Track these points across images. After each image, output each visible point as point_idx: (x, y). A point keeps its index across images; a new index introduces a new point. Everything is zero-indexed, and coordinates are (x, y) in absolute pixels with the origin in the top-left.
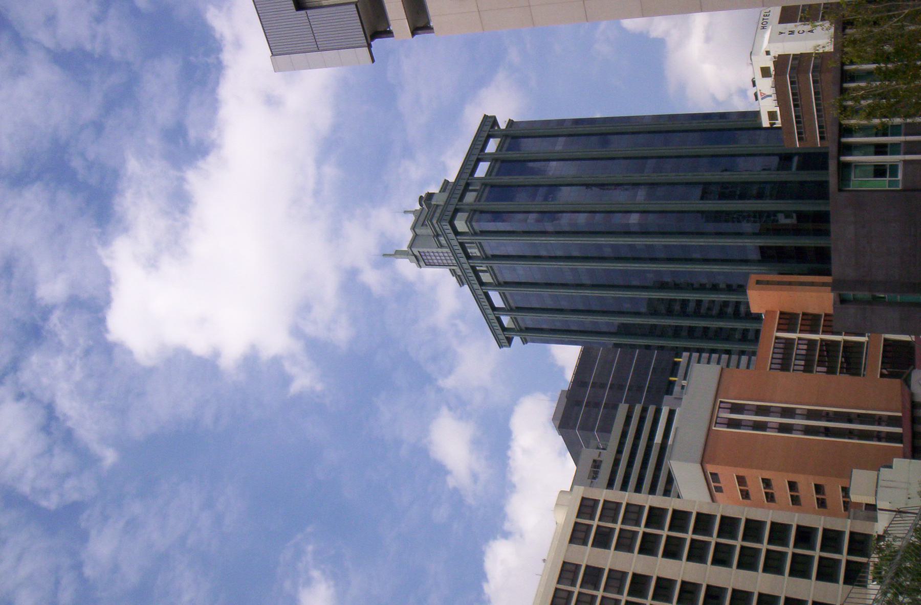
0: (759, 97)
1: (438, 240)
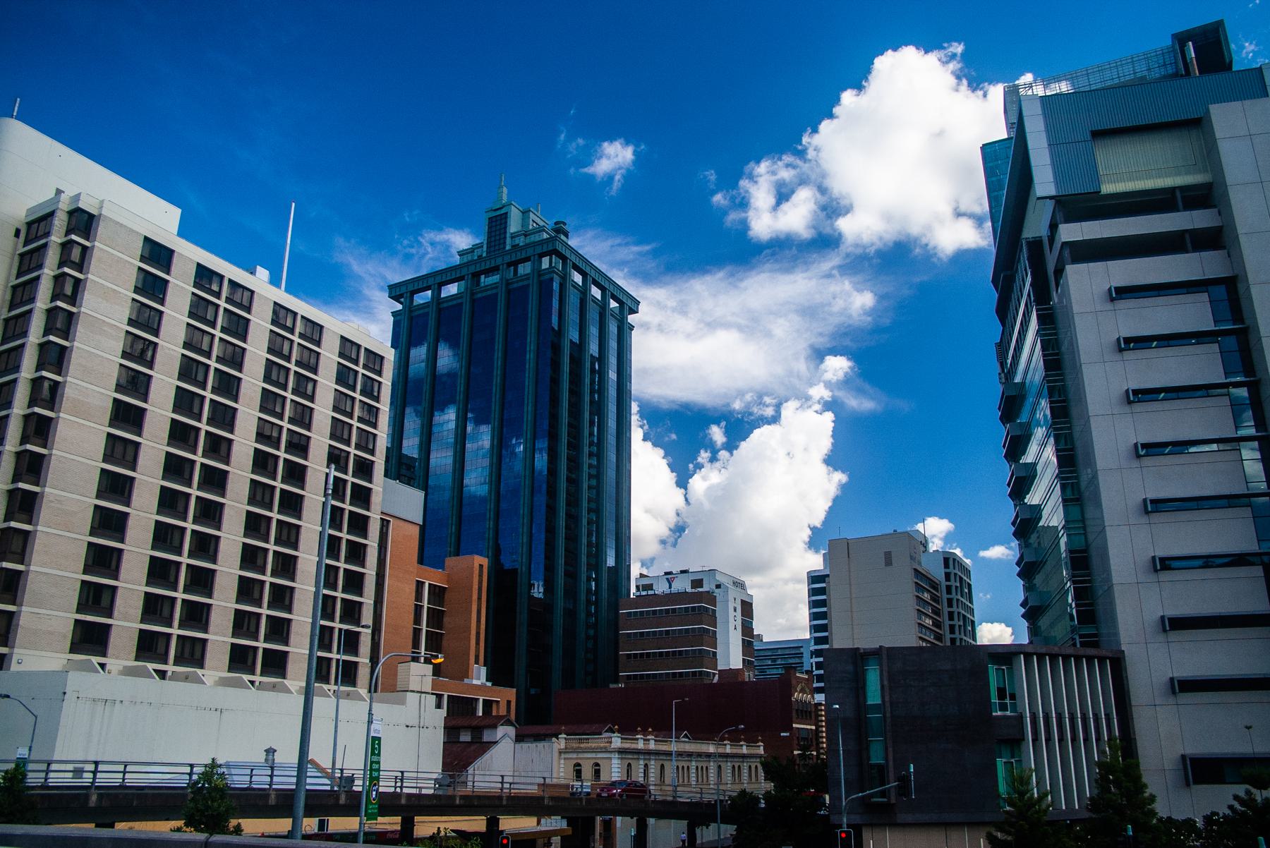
0: (669, 576)
1: (521, 235)
